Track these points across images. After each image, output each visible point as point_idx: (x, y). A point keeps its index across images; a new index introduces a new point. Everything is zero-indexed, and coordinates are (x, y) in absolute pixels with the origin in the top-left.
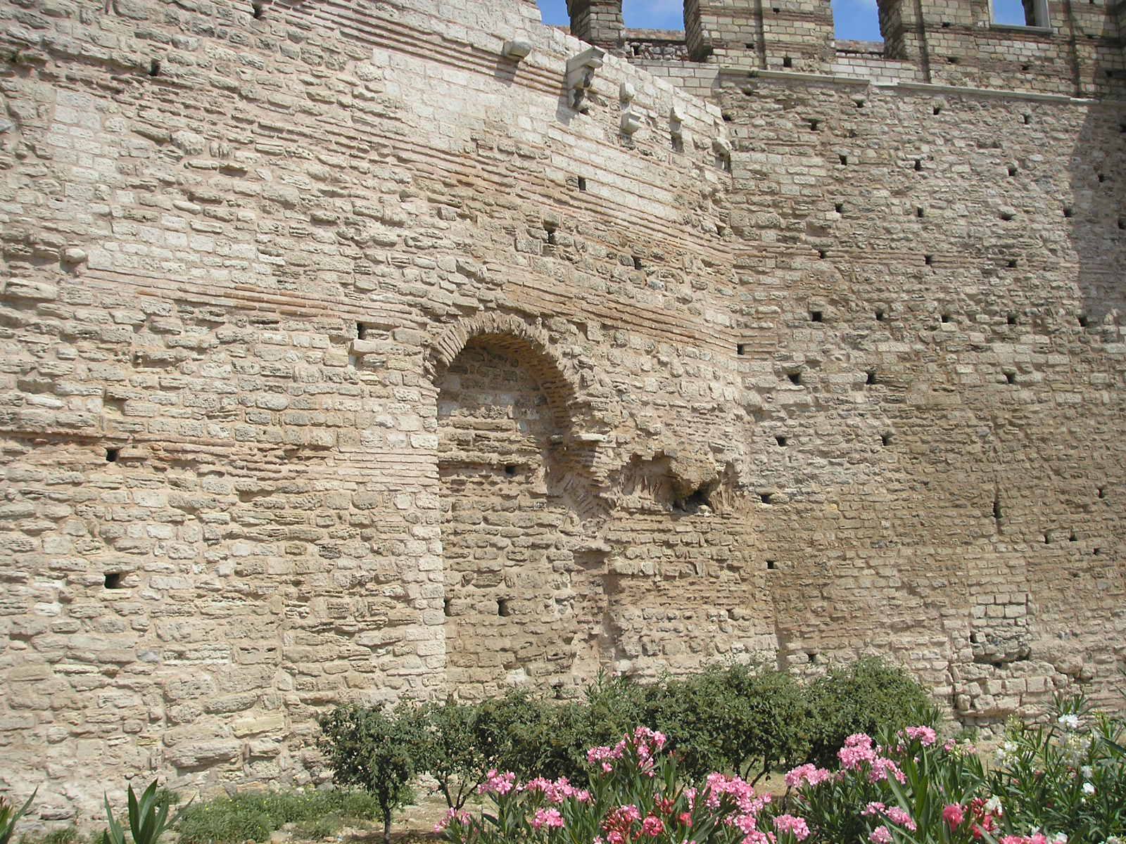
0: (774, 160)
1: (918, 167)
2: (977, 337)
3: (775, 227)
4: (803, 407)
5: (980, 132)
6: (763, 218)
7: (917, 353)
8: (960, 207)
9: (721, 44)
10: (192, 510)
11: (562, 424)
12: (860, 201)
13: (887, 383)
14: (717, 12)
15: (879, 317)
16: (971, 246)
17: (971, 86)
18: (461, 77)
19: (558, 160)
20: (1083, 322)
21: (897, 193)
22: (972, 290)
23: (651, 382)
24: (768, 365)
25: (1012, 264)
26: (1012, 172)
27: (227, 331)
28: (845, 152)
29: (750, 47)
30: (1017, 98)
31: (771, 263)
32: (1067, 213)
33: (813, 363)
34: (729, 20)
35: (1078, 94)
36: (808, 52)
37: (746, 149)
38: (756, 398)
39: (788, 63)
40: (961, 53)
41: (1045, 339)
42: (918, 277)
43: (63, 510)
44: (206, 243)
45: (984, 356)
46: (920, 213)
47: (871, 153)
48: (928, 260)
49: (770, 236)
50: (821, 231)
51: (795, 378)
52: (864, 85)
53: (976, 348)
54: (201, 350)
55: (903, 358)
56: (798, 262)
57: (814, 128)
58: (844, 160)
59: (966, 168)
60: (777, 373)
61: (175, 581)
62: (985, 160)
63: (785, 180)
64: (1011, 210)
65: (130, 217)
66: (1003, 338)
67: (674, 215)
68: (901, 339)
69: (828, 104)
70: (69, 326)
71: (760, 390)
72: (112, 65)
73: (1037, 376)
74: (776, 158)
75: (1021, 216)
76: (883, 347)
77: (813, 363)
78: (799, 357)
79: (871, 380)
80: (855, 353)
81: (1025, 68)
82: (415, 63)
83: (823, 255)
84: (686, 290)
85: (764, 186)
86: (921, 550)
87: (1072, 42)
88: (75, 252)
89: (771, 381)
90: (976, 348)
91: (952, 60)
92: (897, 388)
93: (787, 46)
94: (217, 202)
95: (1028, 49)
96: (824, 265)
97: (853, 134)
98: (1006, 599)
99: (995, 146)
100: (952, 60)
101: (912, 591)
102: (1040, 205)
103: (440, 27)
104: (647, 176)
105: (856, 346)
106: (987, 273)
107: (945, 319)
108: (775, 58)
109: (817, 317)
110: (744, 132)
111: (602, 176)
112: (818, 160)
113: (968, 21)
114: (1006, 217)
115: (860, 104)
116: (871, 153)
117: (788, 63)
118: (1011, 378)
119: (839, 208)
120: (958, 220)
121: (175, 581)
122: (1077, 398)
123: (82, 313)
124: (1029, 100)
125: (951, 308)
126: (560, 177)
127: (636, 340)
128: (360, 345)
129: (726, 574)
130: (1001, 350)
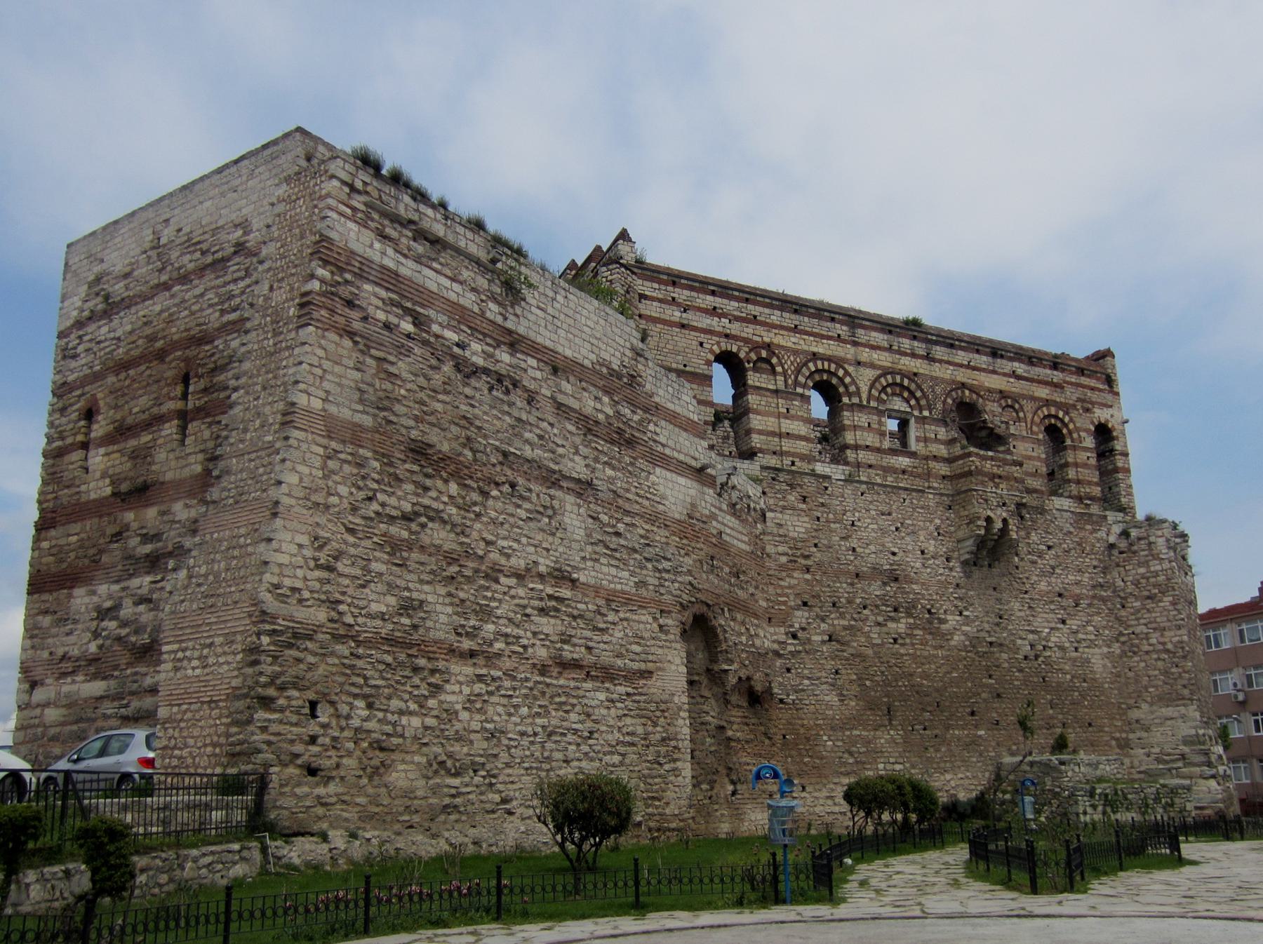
0: (786, 518)
1: (853, 525)
2: (880, 619)
3: (787, 554)
4: (800, 652)
5: (886, 509)
6: (781, 549)
7: (852, 626)
8: (872, 547)
9: (761, 451)
10: (612, 701)
11: (713, 659)
12: (826, 542)
13: (838, 641)
14: (760, 432)
15: (834, 605)
16: (876, 570)
17: (879, 481)
18: (682, 480)
19: (714, 523)
20: (929, 612)
21: (842, 538)
22: (878, 593)
23: (744, 639)
24: (782, 630)
25: (896, 580)
26: (897, 529)
27: (622, 615)
28: (819, 514)
29: (774, 453)
30: (900, 488)
31: (784, 574)
32: (923, 552)
33: (803, 629)
34: (762, 437)
35: (929, 487)
36: (803, 458)
37: (772, 511)
38: (776, 646)
39: (793, 463)
40: (873, 462)
41: (912, 621)
42: (852, 584)
43: (574, 701)
44: (613, 571)
45: (884, 629)
46: (854, 550)
47: (831, 516)
48: (857, 575)
49: (784, 559)
50: (807, 557)
51: (794, 636)
52: (829, 477)
53: (879, 624)
54: (614, 624)
55: (845, 628)
56: (795, 575)
57: (804, 501)
58: (818, 519)
59: (875, 526)
60: (786, 634)
61: (610, 737)
62: (884, 522)
63: (791, 528)
64: (896, 550)
65: (591, 559)
66: (892, 619)
67: (747, 548)
68: (844, 618)
69: (810, 485)
70: (575, 613)
71: (780, 643)
72: (579, 481)
73: (908, 641)
74: (787, 517)
75: (901, 554)
76: (836, 622)
77: (803, 629)
78: (797, 626)
79: (830, 640)
80: (823, 625)
81: (904, 472)
82: (669, 475)
83: (808, 571)
84: (751, 590)
85: (781, 532)
86: (856, 732)
87: (926, 458)
88: (575, 576)
89: (782, 638)
90: (879, 624)
91: (870, 466)
92: (842, 644)
93: (793, 455)
94: (615, 550)
95: (904, 462)
96: (808, 576)
97: (823, 505)
98: (892, 760)
99: (890, 514)
100: (870, 466)
101: (851, 754)
102: (910, 547)
103: (676, 455)
104: (741, 529)
105: (823, 620)
106: (885, 584)
107: (865, 608)
108: (787, 461)
109: (805, 604)
110: (772, 501)
111: (728, 531)
112: (806, 519)
113: (878, 445)
114: (894, 554)
115: (826, 488)
116: (831, 516)
117: (793, 463)
118: (895, 640)
119: (816, 545)
120: (871, 556)
121: (610, 737)
122: (926, 653)
123: (579, 606)
124: (906, 489)
125: (868, 602)
126: (715, 532)
127: (739, 617)
128: (661, 621)
129: (767, 741)
130: (891, 625)
